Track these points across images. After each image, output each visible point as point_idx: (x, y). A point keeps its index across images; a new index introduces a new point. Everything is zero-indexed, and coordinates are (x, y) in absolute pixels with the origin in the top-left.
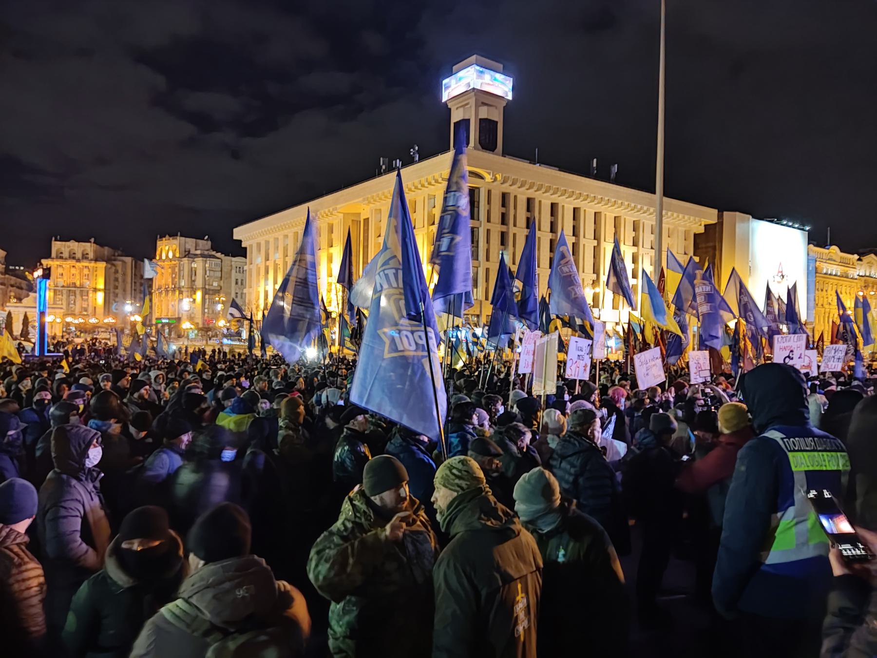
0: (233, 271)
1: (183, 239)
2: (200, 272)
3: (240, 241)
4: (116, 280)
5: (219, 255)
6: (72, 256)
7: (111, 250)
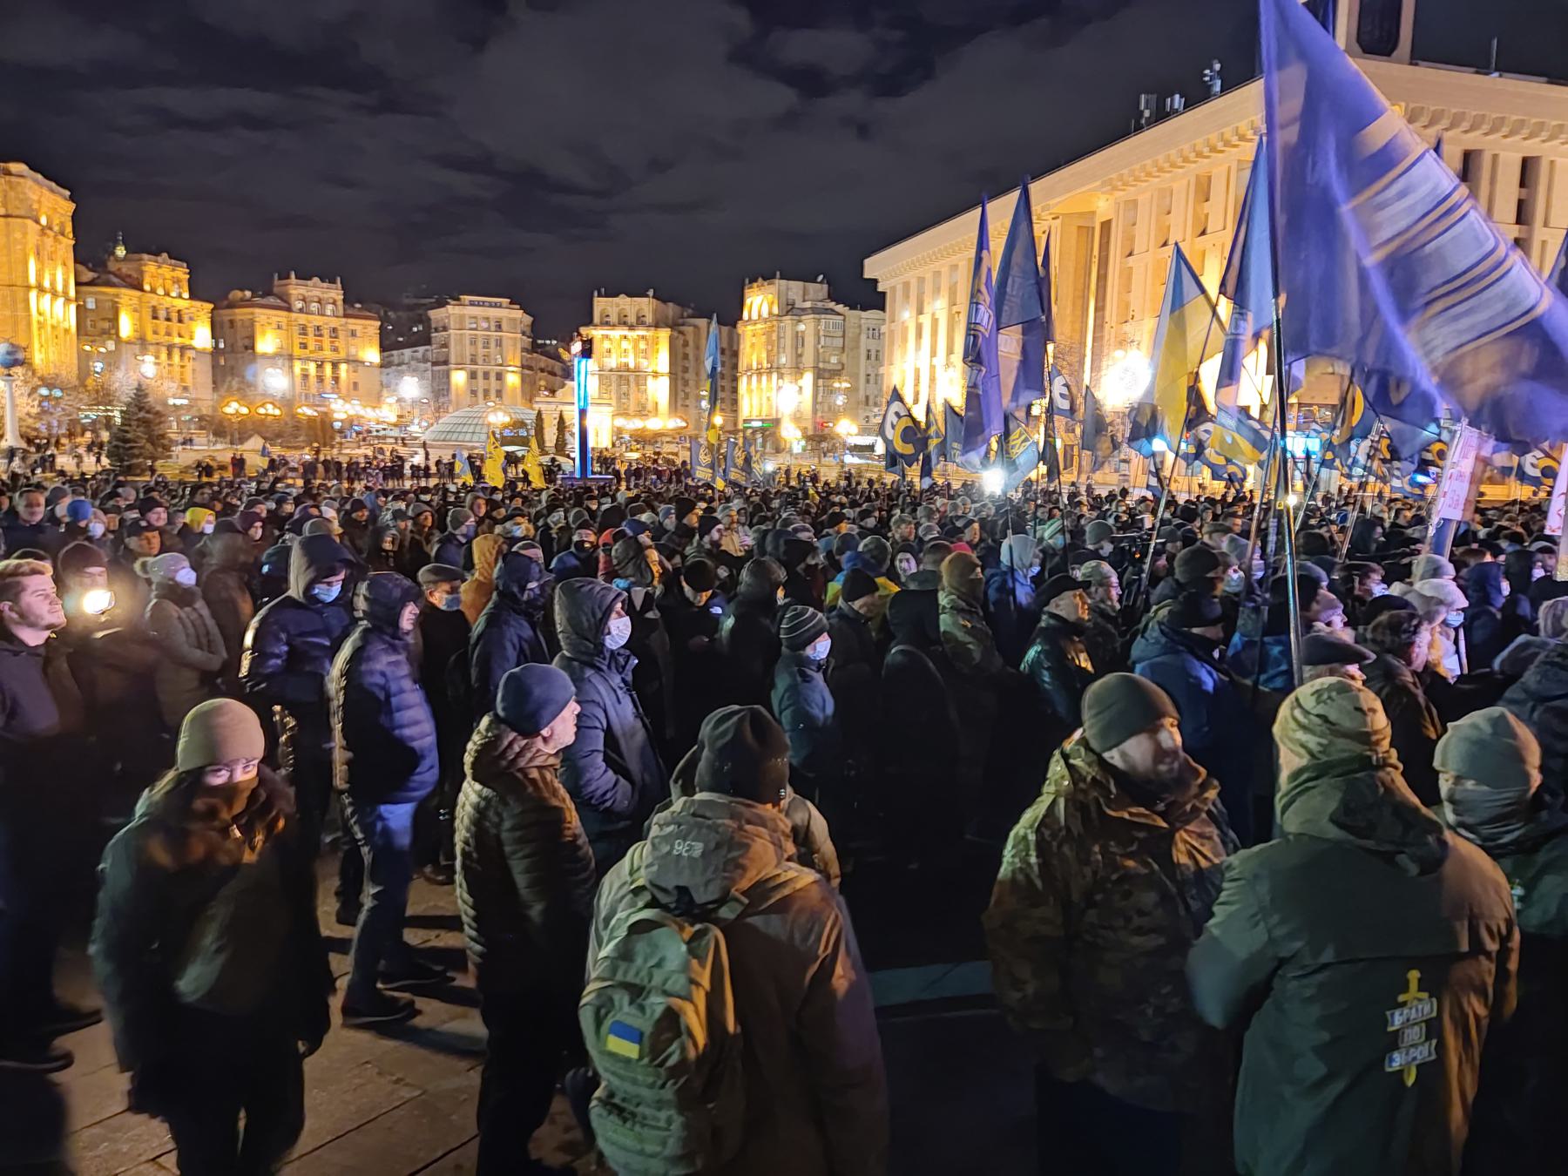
0: (863, 337)
1: (784, 282)
2: (810, 340)
3: (875, 281)
4: (686, 356)
5: (840, 308)
6: (623, 322)
7: (678, 309)
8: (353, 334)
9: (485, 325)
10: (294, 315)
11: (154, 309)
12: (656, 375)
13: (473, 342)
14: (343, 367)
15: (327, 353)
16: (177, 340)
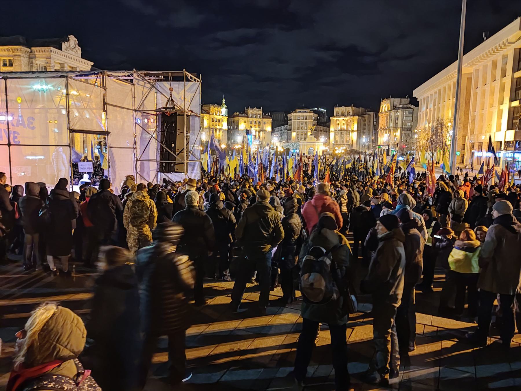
1: (393, 99)
2: (400, 118)
4: (365, 125)
5: (412, 106)
6: (343, 115)
7: (363, 109)
8: (265, 123)
9: (302, 118)
10: (249, 119)
11: (213, 119)
12: (353, 131)
13: (299, 124)
14: (261, 133)
15: (257, 129)
16: (218, 127)
